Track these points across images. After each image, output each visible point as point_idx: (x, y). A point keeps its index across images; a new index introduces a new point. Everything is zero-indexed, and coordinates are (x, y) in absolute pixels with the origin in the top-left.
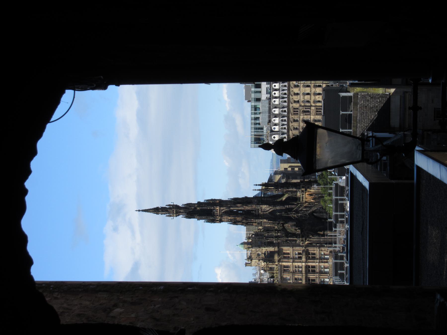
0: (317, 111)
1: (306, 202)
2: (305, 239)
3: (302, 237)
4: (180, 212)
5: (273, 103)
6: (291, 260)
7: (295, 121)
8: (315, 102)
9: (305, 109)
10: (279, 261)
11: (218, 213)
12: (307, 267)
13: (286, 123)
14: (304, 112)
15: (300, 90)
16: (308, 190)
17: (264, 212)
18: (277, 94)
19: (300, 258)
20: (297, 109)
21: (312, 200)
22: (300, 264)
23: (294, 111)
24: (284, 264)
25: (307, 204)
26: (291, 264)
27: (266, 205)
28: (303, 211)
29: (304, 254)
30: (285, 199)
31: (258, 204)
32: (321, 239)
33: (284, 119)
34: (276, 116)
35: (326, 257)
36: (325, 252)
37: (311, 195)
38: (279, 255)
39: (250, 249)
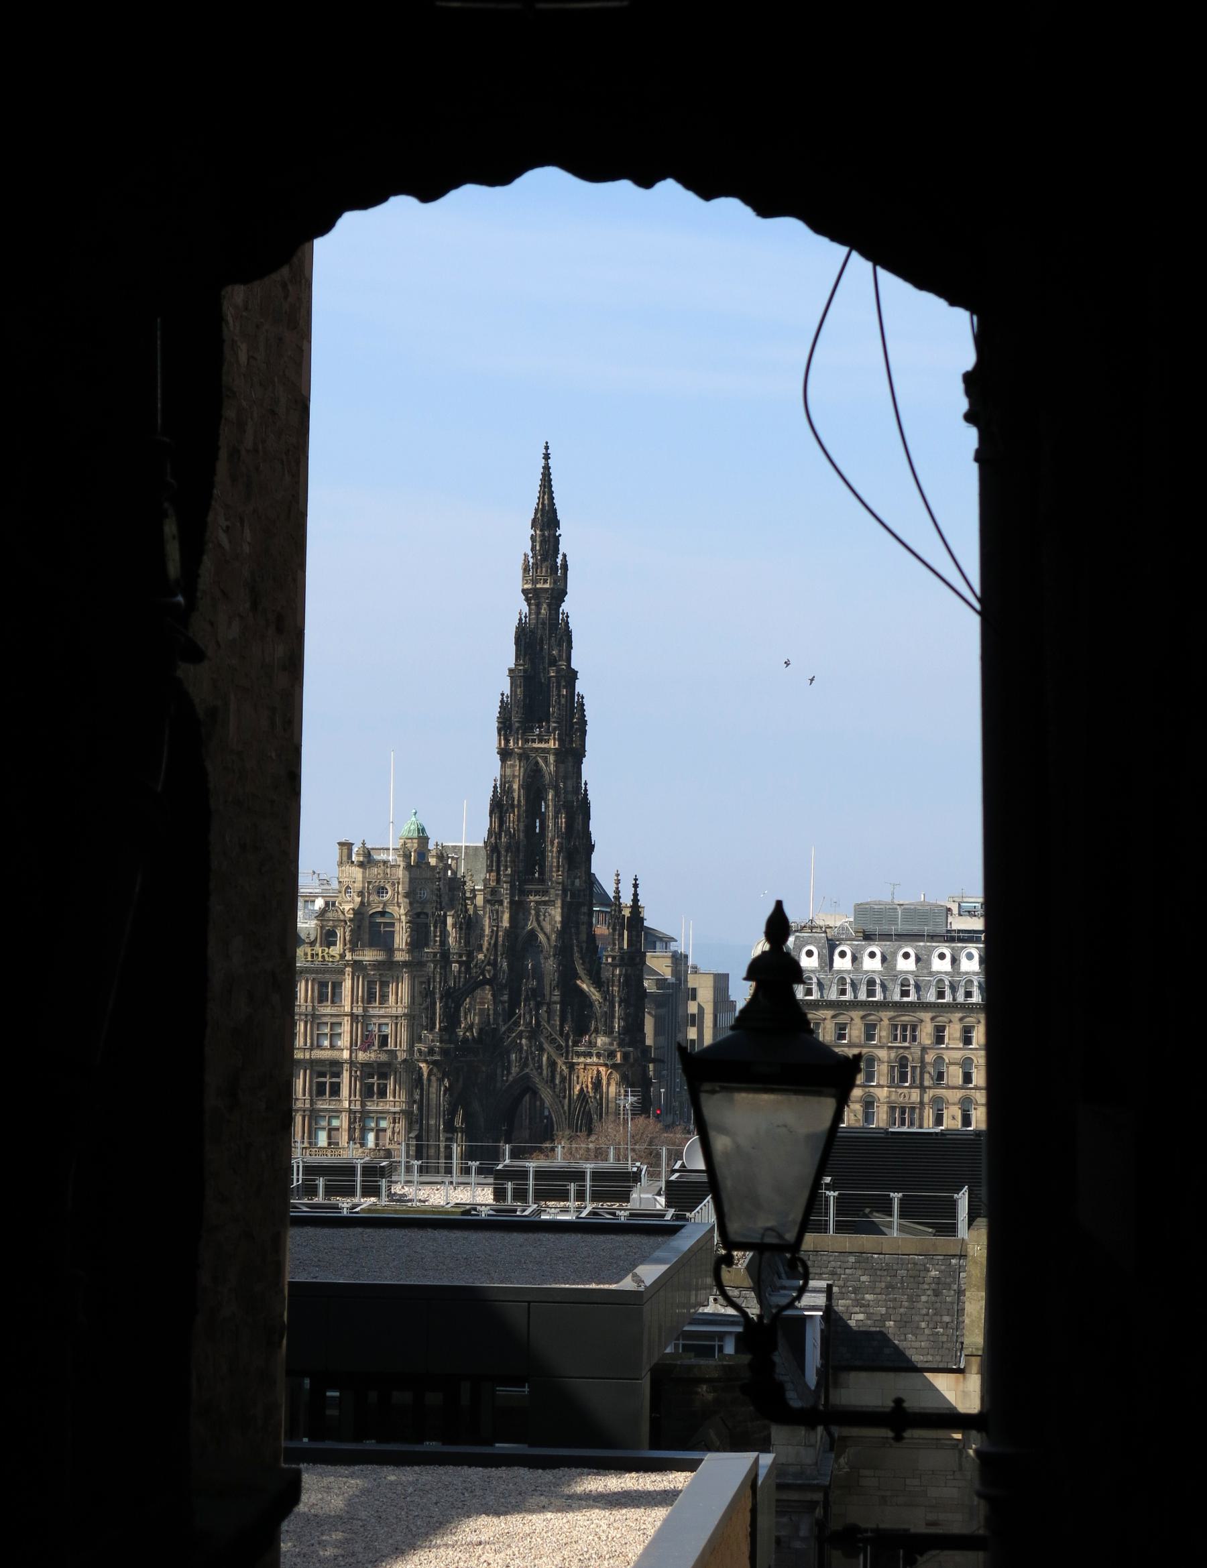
0: (903, 1113)
1: (572, 1067)
3: (444, 1052)
4: (538, 606)
5: (936, 953)
6: (359, 1011)
8: (938, 1103)
9: (914, 1068)
10: (357, 966)
11: (536, 745)
12: (335, 1067)
14: (903, 1062)
17: (537, 915)
20: (914, 1039)
21: (578, 1087)
22: (344, 1042)
23: (904, 1028)
24: (347, 984)
25: (566, 1071)
26: (347, 1009)
27: (562, 922)
28: (540, 1056)
29: (384, 1057)
30: (582, 991)
31: (564, 891)
32: (438, 1117)
33: (878, 989)
35: (371, 1137)
36: (389, 1133)
37: (597, 1084)
38: (378, 965)
39: (401, 862)
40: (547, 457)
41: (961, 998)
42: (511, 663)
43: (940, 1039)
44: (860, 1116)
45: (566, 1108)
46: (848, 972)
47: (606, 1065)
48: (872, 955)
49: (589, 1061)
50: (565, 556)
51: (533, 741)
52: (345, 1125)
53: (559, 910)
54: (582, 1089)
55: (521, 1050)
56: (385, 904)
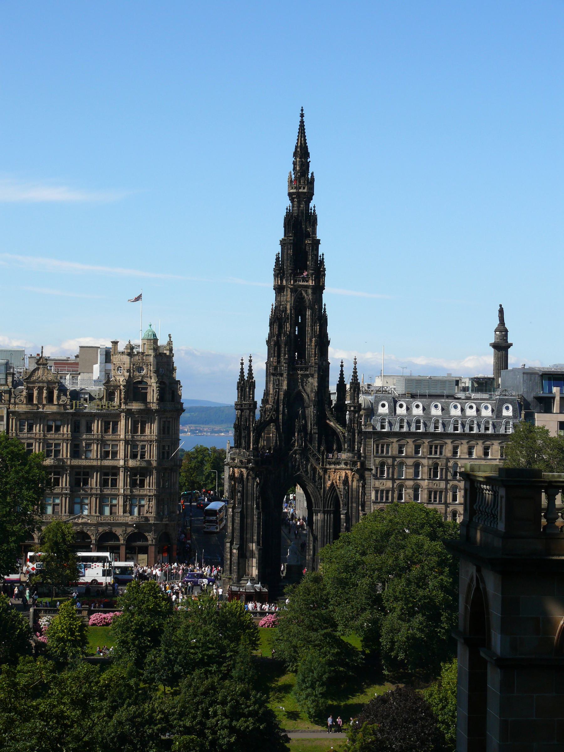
1: (325, 471)
3: (256, 463)
6: (129, 437)
7: (417, 448)
9: (442, 469)
10: (129, 413)
11: (301, 283)
12: (114, 471)
13: (413, 429)
14: (436, 466)
15: (479, 458)
16: (357, 476)
19: (134, 456)
20: (441, 453)
21: (329, 483)
22: (121, 454)
23: (436, 448)
24: (123, 422)
25: (322, 473)
26: (122, 437)
27: (318, 386)
28: (307, 465)
29: (144, 464)
31: (319, 368)
33: (422, 425)
35: (136, 510)
36: (146, 507)
37: (346, 482)
38: (140, 411)
39: (151, 352)
40: (302, 116)
41: (467, 431)
42: (281, 236)
43: (455, 453)
44: (412, 497)
45: (322, 494)
46: (405, 416)
47: (351, 470)
48: (417, 406)
49: (338, 467)
50: (312, 174)
51: (300, 281)
52: (121, 502)
53: (316, 379)
54: (333, 483)
56: (143, 377)
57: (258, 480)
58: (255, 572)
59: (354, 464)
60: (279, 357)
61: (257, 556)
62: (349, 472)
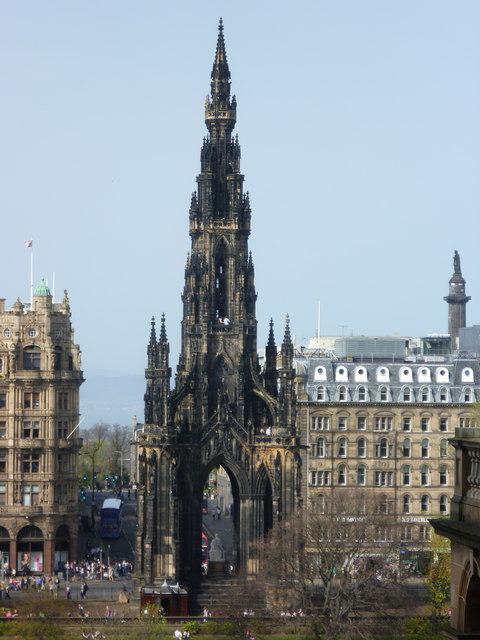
0: (383, 474)
1: (253, 449)
2: (167, 448)
3: (172, 440)
4: (218, 131)
5: (317, 369)
6: (19, 412)
7: (361, 420)
8: (406, 467)
9: (391, 446)
10: (18, 382)
13: (356, 399)
14: (383, 443)
15: (435, 432)
16: (291, 455)
17: (224, 344)
18: (383, 378)
19: (26, 434)
21: (259, 463)
22: (10, 432)
27: (244, 350)
29: (37, 444)
30: (258, 397)
31: (245, 327)
32: (168, 485)
34: (371, 375)
35: (27, 499)
36: (40, 496)
37: (278, 462)
39: (45, 312)
40: (221, 28)
41: (420, 400)
42: (198, 171)
43: (406, 427)
44: (356, 479)
45: (250, 477)
46: (347, 384)
47: (285, 448)
48: (361, 372)
49: (268, 444)
51: (221, 225)
52: (11, 490)
53: (241, 342)
54: (262, 464)
55: (217, 438)
56: (34, 341)
57: (174, 461)
58: (171, 571)
59: (288, 440)
60: (197, 315)
61: (174, 551)
62: (281, 451)
